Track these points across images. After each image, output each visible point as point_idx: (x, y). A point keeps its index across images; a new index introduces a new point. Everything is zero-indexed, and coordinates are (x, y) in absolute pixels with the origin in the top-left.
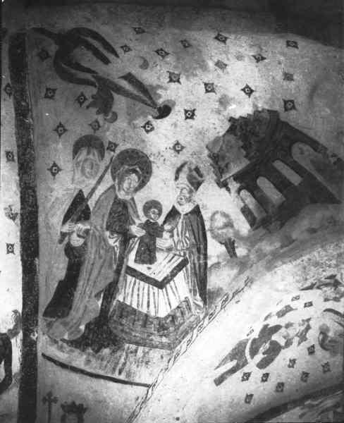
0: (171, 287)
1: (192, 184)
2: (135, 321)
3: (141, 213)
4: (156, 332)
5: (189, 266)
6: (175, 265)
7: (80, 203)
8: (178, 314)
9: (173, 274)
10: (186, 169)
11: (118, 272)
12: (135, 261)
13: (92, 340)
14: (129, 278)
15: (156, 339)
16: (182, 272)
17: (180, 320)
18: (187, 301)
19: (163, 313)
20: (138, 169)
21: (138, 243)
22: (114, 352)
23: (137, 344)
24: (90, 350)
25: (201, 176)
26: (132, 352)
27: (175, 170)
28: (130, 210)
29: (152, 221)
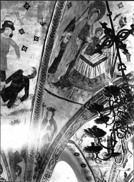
0: (98, 68)
1: (120, 25)
2: (79, 78)
3: (94, 32)
4: (87, 84)
5: (108, 60)
6: (102, 58)
8: (99, 79)
9: (99, 62)
10: (120, 17)
11: (76, 56)
12: (85, 53)
13: (61, 84)
14: (80, 60)
15: (87, 87)
16: (104, 62)
17: (99, 82)
18: (104, 74)
19: (92, 77)
20: (99, 11)
21: (88, 45)
22: (68, 89)
23: (79, 87)
24: (60, 87)
25: (126, 22)
26: (76, 90)
27: (115, 16)
28: (90, 30)
29: (97, 37)
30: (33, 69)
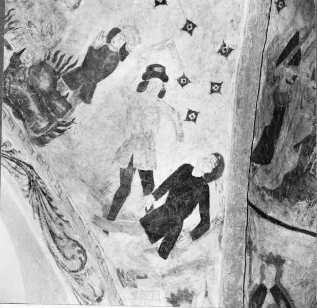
7: (294, 46)
22: (310, 205)
30: (214, 159)
